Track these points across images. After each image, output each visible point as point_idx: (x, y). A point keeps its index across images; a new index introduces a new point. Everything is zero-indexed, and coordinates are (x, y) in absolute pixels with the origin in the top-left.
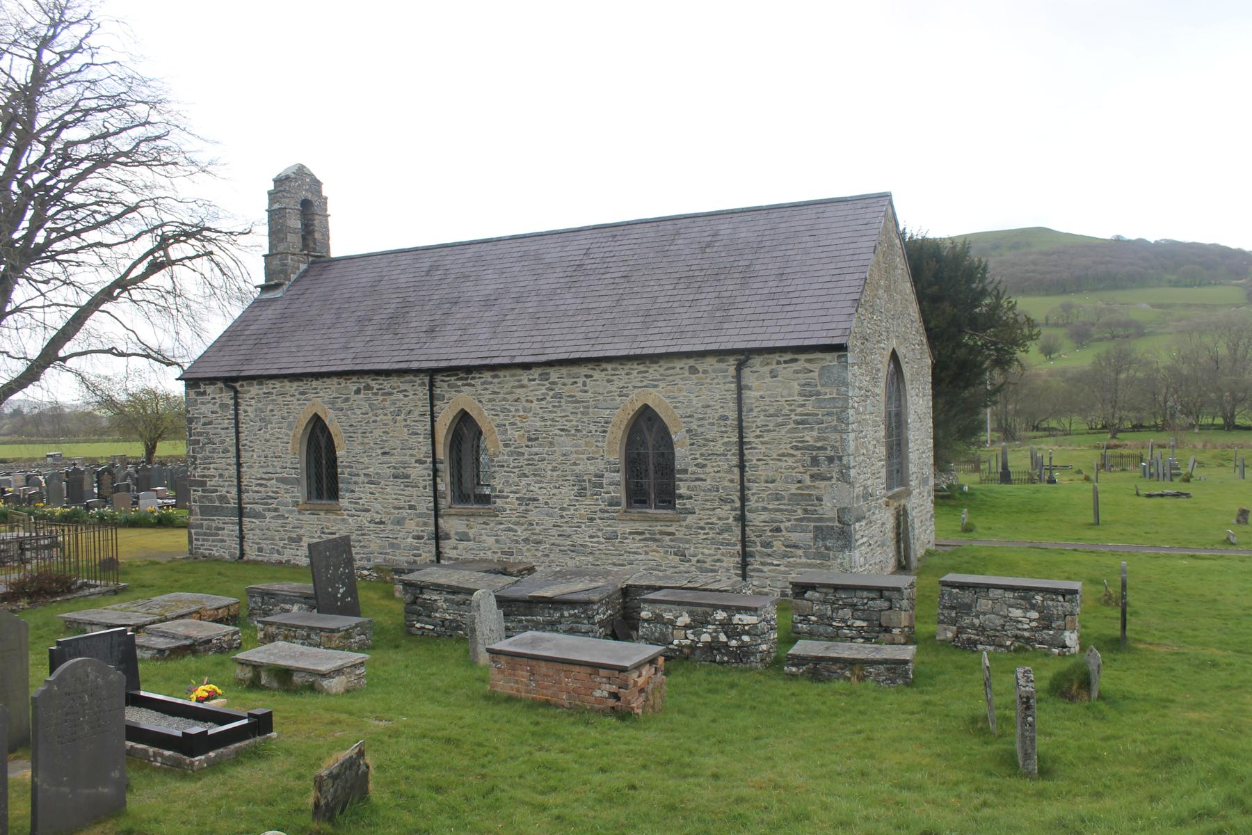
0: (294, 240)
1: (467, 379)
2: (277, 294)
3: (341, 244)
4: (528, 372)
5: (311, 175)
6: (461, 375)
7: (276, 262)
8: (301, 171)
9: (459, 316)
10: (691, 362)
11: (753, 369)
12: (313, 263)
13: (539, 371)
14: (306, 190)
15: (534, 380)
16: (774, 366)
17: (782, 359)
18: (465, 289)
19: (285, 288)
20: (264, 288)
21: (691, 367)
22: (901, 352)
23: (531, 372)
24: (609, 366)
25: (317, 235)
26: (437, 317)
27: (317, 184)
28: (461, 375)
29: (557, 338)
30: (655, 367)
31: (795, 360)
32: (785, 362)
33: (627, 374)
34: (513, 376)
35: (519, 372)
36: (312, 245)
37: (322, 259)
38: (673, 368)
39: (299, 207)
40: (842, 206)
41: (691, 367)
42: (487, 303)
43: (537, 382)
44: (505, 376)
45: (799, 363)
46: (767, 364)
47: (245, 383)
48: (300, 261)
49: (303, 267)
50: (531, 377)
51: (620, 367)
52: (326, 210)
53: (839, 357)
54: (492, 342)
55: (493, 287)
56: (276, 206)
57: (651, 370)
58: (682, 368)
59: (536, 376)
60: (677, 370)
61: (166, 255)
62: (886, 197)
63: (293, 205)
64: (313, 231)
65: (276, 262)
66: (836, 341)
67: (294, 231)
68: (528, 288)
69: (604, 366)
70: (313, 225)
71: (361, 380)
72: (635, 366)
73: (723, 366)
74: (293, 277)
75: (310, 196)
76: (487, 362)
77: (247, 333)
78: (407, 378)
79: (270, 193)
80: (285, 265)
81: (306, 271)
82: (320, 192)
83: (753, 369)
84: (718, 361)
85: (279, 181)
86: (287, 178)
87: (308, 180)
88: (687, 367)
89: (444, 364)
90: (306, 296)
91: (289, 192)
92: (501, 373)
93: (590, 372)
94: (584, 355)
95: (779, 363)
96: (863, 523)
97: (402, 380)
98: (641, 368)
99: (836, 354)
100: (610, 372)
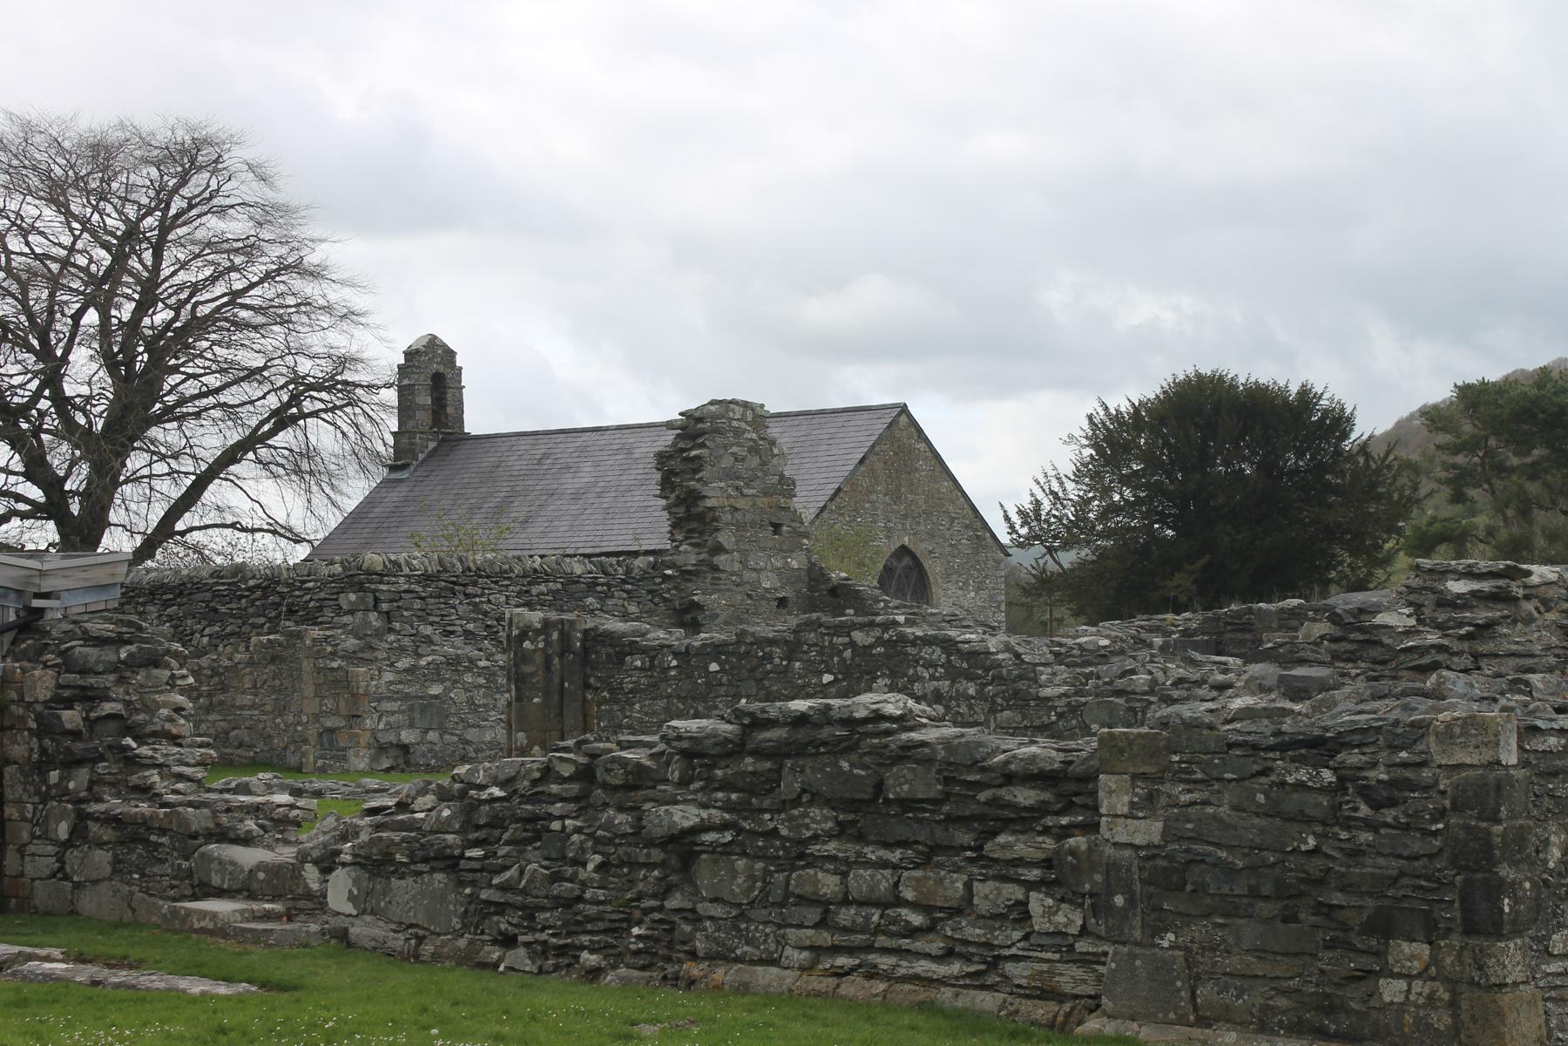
0: (424, 418)
2: (404, 475)
3: (476, 421)
5: (444, 346)
7: (405, 440)
8: (433, 343)
9: (551, 508)
12: (443, 440)
14: (438, 363)
18: (563, 481)
19: (412, 468)
20: (392, 468)
22: (920, 549)
25: (450, 410)
26: (533, 508)
27: (450, 354)
29: (615, 532)
36: (443, 420)
37: (452, 437)
39: (429, 382)
40: (865, 415)
42: (576, 496)
48: (428, 440)
49: (432, 445)
52: (460, 381)
54: (568, 534)
55: (586, 480)
56: (406, 382)
61: (300, 410)
63: (422, 380)
64: (445, 406)
65: (405, 440)
67: (424, 408)
68: (612, 483)
70: (445, 399)
74: (421, 456)
75: (441, 369)
77: (371, 515)
79: (399, 367)
80: (413, 444)
81: (435, 450)
82: (453, 362)
85: (410, 354)
86: (417, 352)
90: (431, 478)
91: (419, 367)
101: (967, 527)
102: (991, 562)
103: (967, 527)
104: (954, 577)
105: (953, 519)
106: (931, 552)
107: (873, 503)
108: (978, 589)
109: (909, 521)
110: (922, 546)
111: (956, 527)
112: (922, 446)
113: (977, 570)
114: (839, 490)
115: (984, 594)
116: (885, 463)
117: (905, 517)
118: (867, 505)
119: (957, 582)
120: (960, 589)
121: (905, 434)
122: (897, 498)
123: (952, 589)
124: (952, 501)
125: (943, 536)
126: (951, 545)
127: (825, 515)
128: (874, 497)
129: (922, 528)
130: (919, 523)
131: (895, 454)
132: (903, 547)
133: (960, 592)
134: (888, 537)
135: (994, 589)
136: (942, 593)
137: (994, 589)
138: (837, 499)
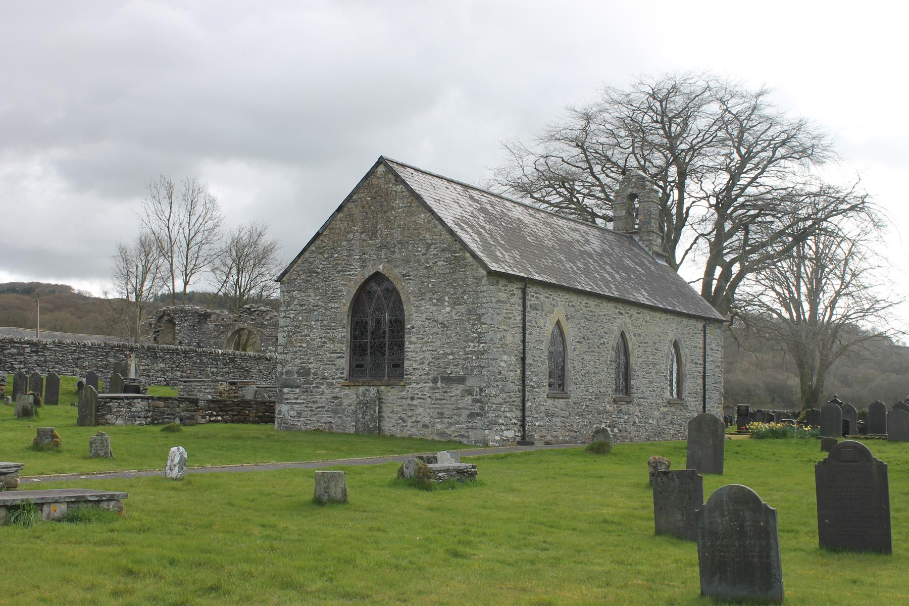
22: (394, 274)
62: (381, 161)
87: (634, 180)
96: (298, 390)
101: (443, 250)
102: (471, 279)
103: (443, 250)
104: (429, 295)
105: (428, 246)
106: (404, 276)
107: (349, 241)
108: (455, 304)
109: (384, 251)
110: (396, 271)
111: (433, 251)
112: (399, 188)
113: (455, 288)
114: (318, 235)
115: (462, 309)
116: (363, 207)
117: (380, 249)
118: (344, 243)
119: (431, 299)
120: (435, 305)
121: (382, 180)
122: (373, 234)
123: (425, 305)
124: (428, 230)
125: (419, 261)
126: (427, 268)
127: (307, 254)
128: (350, 236)
129: (397, 256)
130: (394, 252)
131: (373, 198)
132: (378, 274)
133: (435, 308)
134: (363, 267)
135: (473, 303)
136: (414, 309)
137: (473, 303)
138: (317, 242)
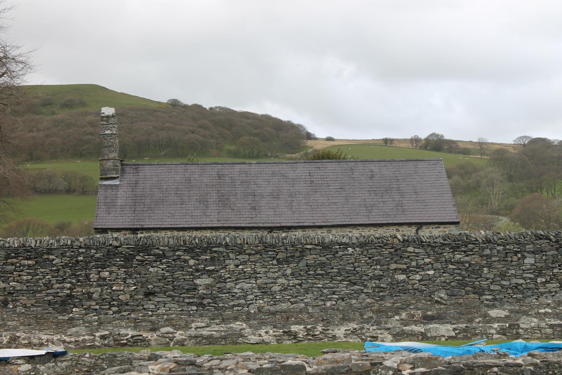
1: (288, 232)
4: (321, 229)
6: (285, 230)
10: (397, 227)
11: (423, 230)
13: (327, 229)
15: (324, 233)
16: (431, 230)
17: (434, 227)
21: (397, 229)
23: (323, 229)
24: (360, 228)
28: (285, 230)
30: (381, 228)
31: (439, 227)
32: (435, 228)
33: (369, 231)
34: (313, 231)
35: (316, 229)
38: (389, 229)
41: (397, 229)
43: (325, 234)
44: (309, 231)
45: (441, 228)
46: (428, 228)
47: (144, 232)
50: (322, 232)
51: (365, 228)
53: (456, 226)
57: (379, 230)
58: (393, 229)
59: (325, 231)
60: (391, 230)
66: (456, 220)
69: (358, 228)
71: (225, 231)
72: (372, 228)
73: (410, 229)
76: (301, 224)
78: (254, 231)
83: (423, 230)
84: (408, 227)
88: (395, 229)
89: (278, 225)
92: (307, 230)
93: (351, 230)
94: (347, 223)
95: (433, 228)
97: (251, 232)
98: (375, 229)
99: (455, 226)
100: (361, 230)
